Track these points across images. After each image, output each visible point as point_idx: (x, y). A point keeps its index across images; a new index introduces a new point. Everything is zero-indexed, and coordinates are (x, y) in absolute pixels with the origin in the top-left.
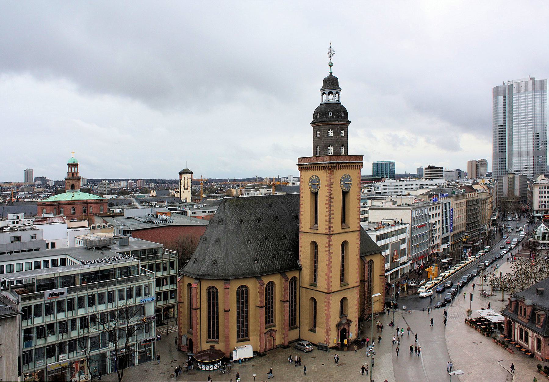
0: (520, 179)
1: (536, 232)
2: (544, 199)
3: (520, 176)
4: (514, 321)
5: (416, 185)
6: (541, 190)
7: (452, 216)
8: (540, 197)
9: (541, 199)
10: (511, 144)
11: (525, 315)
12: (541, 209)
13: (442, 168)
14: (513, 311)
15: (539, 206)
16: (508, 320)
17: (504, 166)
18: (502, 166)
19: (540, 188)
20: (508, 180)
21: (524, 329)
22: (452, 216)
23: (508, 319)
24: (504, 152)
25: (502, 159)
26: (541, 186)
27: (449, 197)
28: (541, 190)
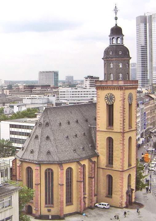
5: (87, 91)
10: (151, 60)
13: (98, 78)
17: (146, 78)
18: (144, 78)
22: (145, 118)
25: (144, 72)
27: (143, 104)
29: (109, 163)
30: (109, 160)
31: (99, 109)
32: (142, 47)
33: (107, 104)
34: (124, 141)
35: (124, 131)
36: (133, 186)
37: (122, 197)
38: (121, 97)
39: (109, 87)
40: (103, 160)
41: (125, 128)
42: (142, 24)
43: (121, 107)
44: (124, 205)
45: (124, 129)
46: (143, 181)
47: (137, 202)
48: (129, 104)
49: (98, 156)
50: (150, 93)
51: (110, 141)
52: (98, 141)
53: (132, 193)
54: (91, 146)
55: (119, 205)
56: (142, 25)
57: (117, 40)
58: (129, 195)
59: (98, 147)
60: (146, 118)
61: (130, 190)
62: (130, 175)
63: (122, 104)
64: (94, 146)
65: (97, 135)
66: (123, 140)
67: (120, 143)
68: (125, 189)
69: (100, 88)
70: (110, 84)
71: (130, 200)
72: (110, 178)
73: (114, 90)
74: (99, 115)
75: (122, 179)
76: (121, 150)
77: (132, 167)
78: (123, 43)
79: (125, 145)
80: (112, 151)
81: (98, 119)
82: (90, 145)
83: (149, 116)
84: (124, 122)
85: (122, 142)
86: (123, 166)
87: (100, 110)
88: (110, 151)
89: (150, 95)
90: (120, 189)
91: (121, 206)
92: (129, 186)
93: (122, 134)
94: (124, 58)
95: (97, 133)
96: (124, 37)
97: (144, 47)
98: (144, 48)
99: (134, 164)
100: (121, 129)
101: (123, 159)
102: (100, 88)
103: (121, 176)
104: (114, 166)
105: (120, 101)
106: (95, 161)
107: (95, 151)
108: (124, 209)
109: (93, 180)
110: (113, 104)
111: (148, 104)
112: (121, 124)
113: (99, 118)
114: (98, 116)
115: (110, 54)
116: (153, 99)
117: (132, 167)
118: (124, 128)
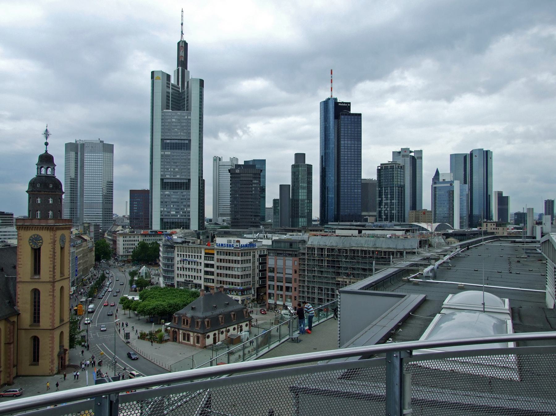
0: (95, 228)
1: (140, 273)
2: (127, 246)
3: (94, 225)
4: (179, 329)
6: (125, 239)
7: (76, 263)
8: (124, 245)
9: (125, 247)
10: (82, 195)
11: (187, 324)
12: (125, 254)
14: (177, 324)
15: (124, 252)
16: (173, 330)
19: (124, 238)
20: (84, 229)
21: (187, 332)
22: (76, 263)
23: (173, 329)
24: (76, 203)
26: (124, 235)
27: (74, 247)
28: (125, 239)
29: (35, 321)
30: (35, 317)
31: (21, 254)
32: (72, 179)
33: (32, 248)
34: (55, 292)
35: (54, 279)
36: (66, 345)
37: (52, 362)
38: (51, 239)
39: (34, 227)
40: (26, 317)
41: (55, 276)
42: (72, 152)
43: (50, 251)
44: (55, 371)
45: (54, 278)
46: (78, 337)
47: (72, 364)
48: (61, 247)
49: (19, 314)
50: (82, 234)
51: (36, 293)
52: (19, 295)
53: (65, 354)
54: (9, 302)
55: (48, 372)
56: (73, 154)
57: (47, 170)
58: (62, 358)
59: (18, 302)
60: (78, 263)
61: (62, 350)
62: (62, 333)
63: (52, 247)
64: (12, 301)
65: (17, 287)
66: (54, 290)
67: (50, 295)
68: (57, 350)
69: (22, 227)
70: (36, 222)
71: (63, 363)
72: (36, 340)
73: (41, 231)
74: (20, 261)
75: (53, 338)
76: (50, 303)
77: (64, 322)
78: (54, 175)
79: (55, 296)
80: (39, 306)
81: (20, 267)
82: (7, 301)
83: (81, 261)
84: (54, 269)
85: (52, 294)
86: (53, 322)
87: (22, 255)
88: (35, 306)
89: (83, 236)
90: (50, 351)
91: (51, 374)
92: (61, 346)
93: (52, 283)
94: (56, 192)
95: (17, 284)
96: (56, 168)
97: (74, 179)
98: (73, 180)
99: (66, 318)
100: (50, 278)
101: (54, 314)
102: (22, 227)
103: (51, 335)
104: (41, 324)
105: (49, 243)
106: (14, 322)
107: (14, 309)
108: (56, 376)
109: (12, 346)
110: (40, 248)
111: (80, 246)
112: (50, 271)
113: (20, 266)
114: (19, 263)
115: (38, 186)
116: (86, 240)
117: (64, 322)
118: (54, 276)
